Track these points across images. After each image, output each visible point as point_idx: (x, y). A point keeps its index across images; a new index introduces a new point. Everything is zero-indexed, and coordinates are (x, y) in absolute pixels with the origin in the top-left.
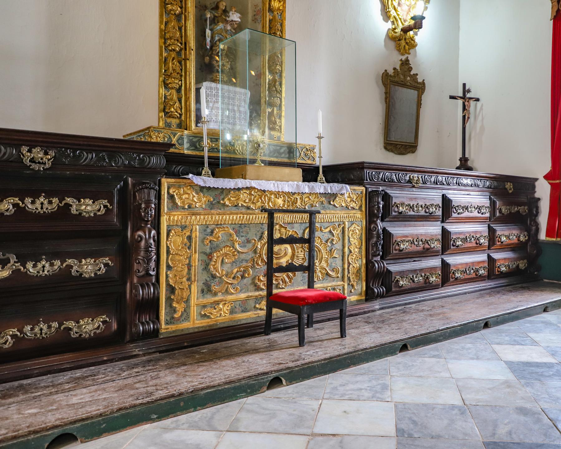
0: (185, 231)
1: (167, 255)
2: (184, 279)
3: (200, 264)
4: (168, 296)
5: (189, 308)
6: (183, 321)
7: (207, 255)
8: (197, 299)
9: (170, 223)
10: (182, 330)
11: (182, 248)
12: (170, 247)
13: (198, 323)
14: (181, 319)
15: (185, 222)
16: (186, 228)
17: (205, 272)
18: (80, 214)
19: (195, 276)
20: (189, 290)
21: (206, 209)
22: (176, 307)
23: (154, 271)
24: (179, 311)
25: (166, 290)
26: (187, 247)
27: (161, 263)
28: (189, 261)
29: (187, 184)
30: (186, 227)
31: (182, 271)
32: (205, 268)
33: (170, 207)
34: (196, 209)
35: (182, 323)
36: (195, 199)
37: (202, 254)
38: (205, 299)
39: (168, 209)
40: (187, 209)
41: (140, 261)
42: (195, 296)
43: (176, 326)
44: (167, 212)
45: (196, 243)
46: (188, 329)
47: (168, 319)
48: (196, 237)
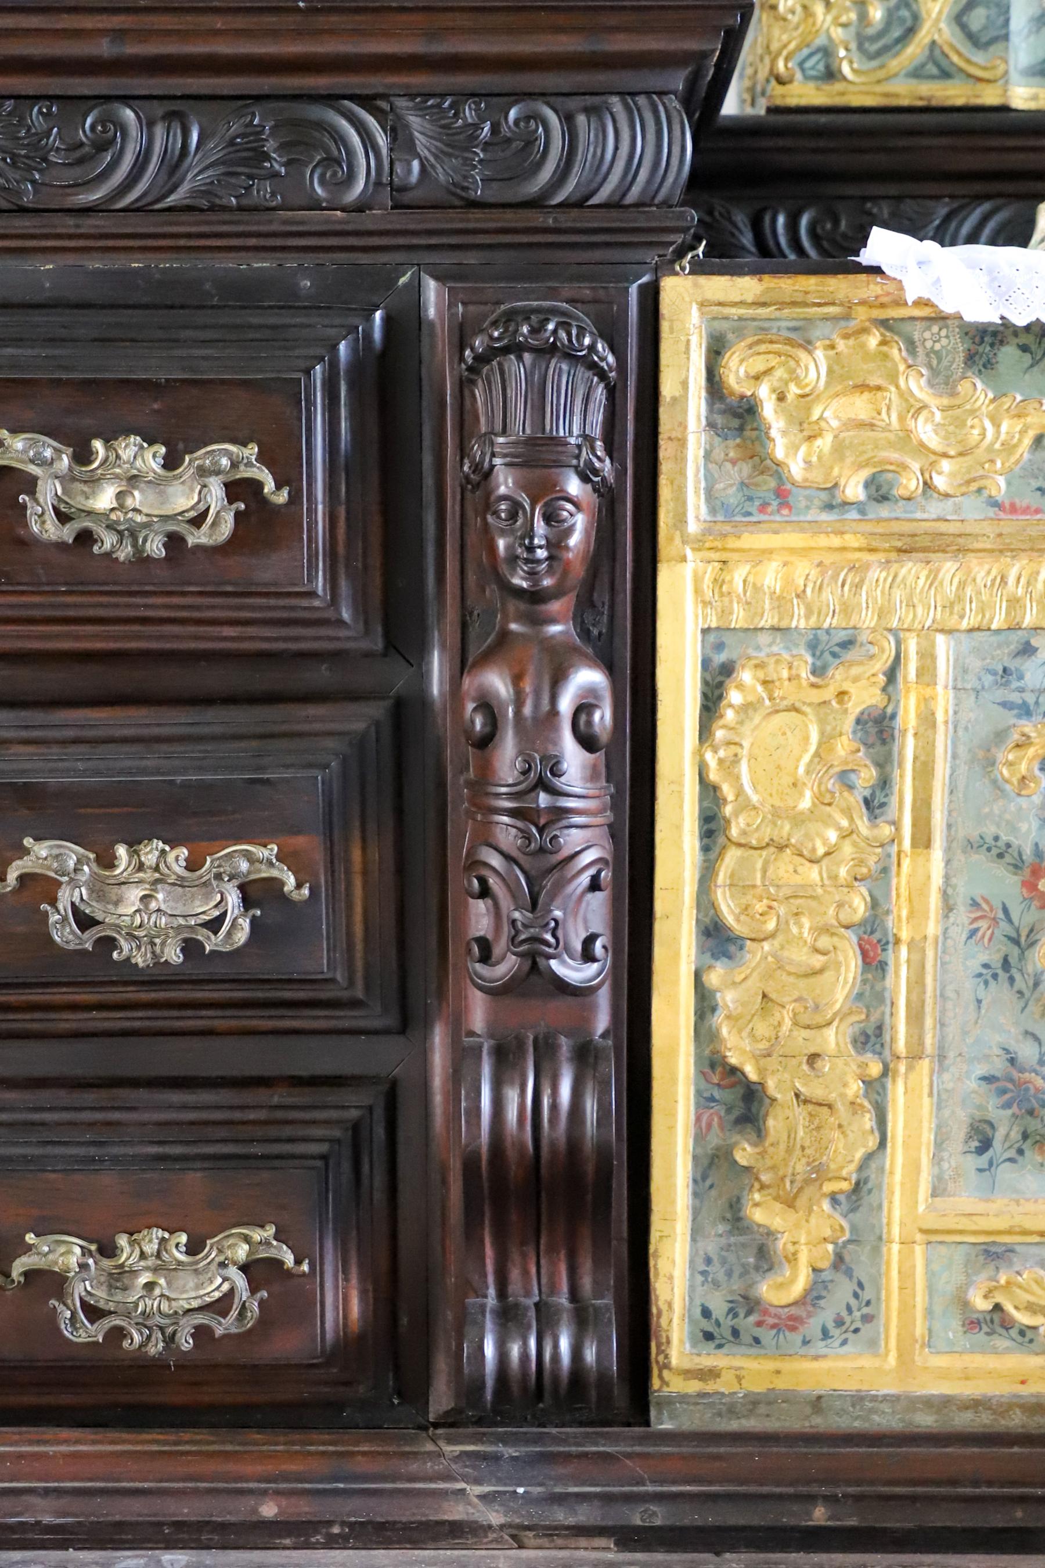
0: (838, 677)
1: (706, 849)
2: (832, 1039)
3: (959, 934)
4: (715, 1139)
5: (876, 1251)
6: (825, 1334)
7: (1017, 867)
8: (936, 1192)
9: (725, 613)
10: (817, 1403)
11: (823, 800)
12: (727, 790)
13: (944, 1374)
14: (813, 1326)
15: (847, 609)
16: (851, 655)
17: (1000, 992)
18: (85, 538)
19: (916, 1017)
20: (868, 1121)
21: (1013, 509)
22: (770, 1234)
23: (588, 956)
24: (792, 1259)
25: (704, 1101)
26: (855, 800)
27: (660, 906)
28: (875, 904)
29: (862, 314)
30: (847, 644)
31: (821, 971)
32: (1006, 964)
33: (732, 496)
34: (935, 508)
35: (820, 1348)
36: (926, 432)
37: (979, 858)
38: (999, 1203)
39: (713, 511)
40: (861, 507)
41: (492, 881)
42: (913, 1168)
43: (770, 1365)
44: (707, 532)
45: (924, 771)
46: (858, 1399)
47: (719, 1306)
48: (928, 720)
